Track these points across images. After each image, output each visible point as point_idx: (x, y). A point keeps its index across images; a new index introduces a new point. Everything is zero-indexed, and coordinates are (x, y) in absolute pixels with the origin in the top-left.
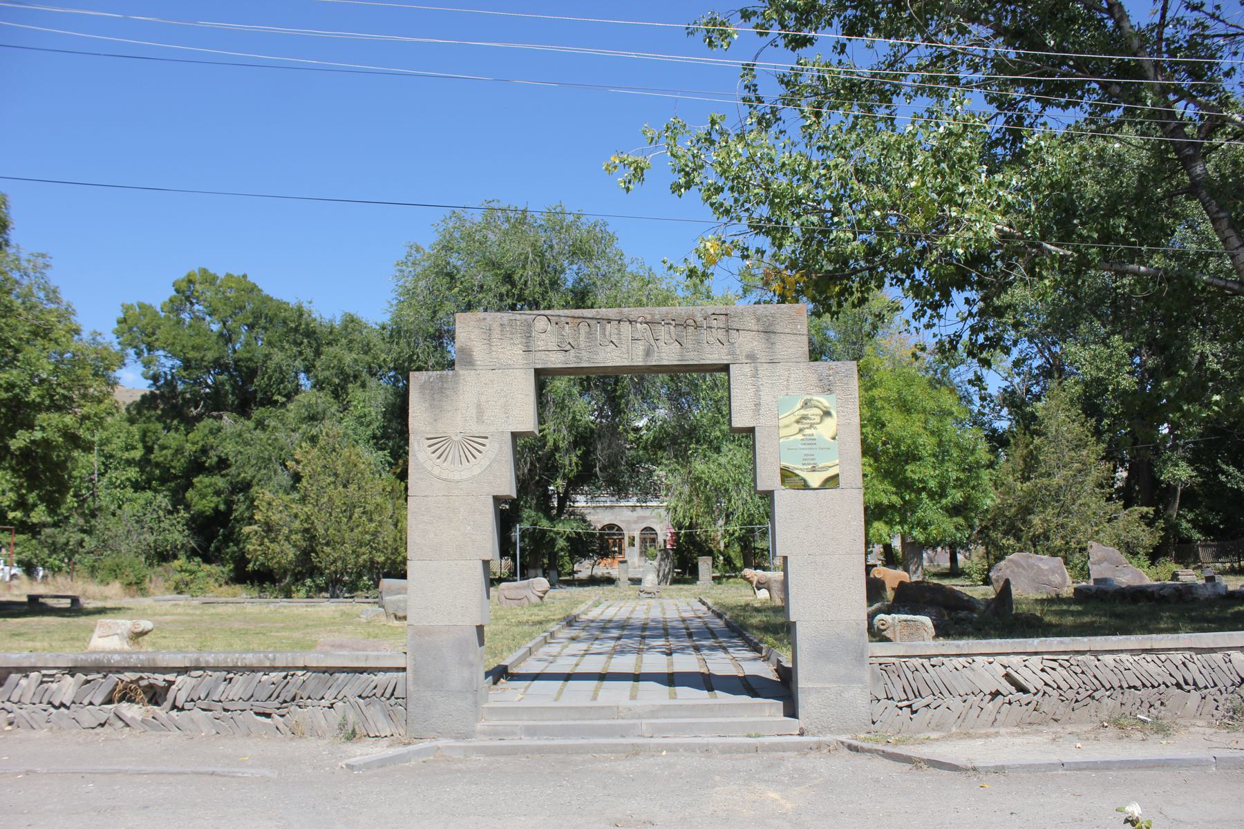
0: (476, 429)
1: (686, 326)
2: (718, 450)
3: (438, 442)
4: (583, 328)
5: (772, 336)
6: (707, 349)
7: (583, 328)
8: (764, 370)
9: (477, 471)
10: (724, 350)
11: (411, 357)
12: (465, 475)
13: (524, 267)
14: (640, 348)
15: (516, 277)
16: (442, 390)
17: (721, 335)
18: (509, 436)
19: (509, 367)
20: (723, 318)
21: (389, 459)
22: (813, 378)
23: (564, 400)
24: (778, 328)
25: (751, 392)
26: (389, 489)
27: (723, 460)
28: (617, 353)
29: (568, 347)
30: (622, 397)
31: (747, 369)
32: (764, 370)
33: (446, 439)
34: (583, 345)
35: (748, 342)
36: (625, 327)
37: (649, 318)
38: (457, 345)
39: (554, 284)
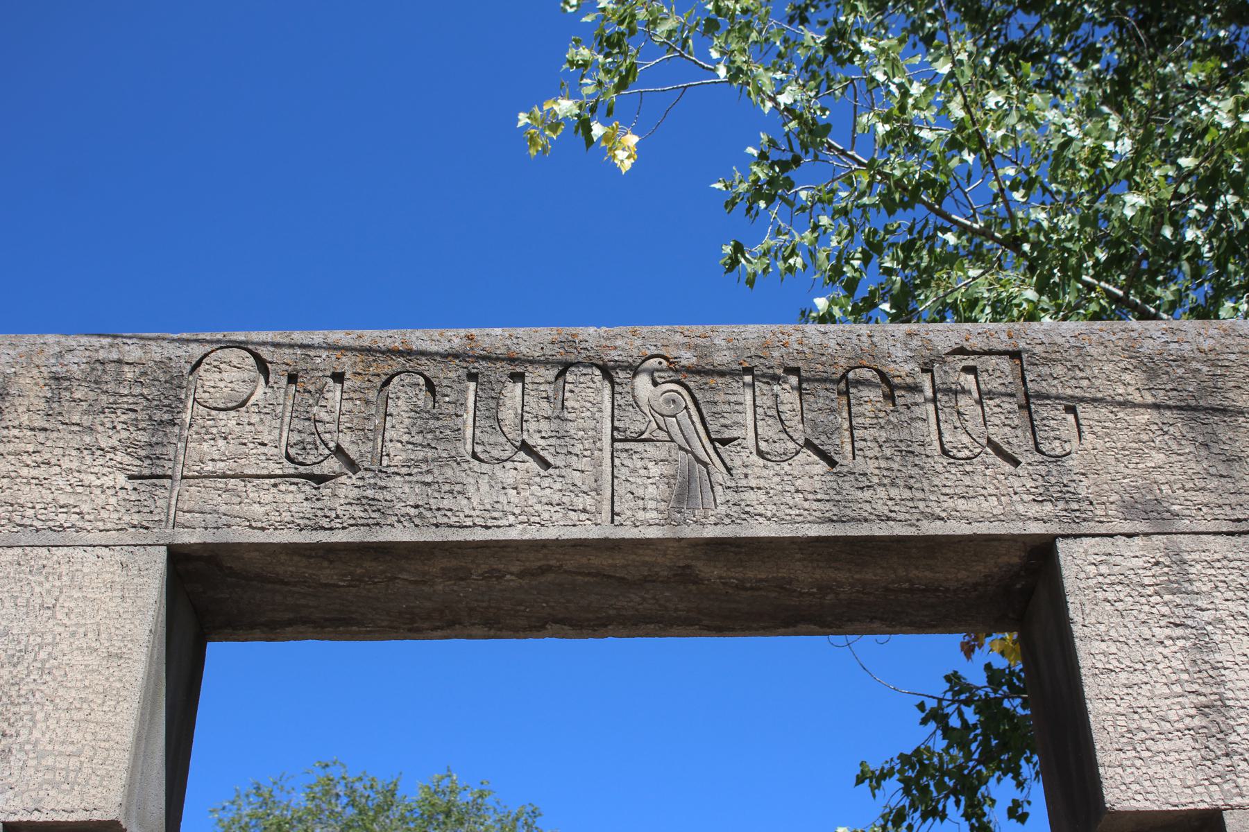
1: (845, 385)
4: (405, 398)
6: (949, 477)
7: (405, 398)
10: (1024, 480)
17: (1003, 424)
19: (54, 536)
20: (1005, 364)
25: (1173, 655)
28: (551, 488)
29: (332, 465)
31: (1134, 556)
34: (398, 454)
36: (590, 396)
37: (687, 358)
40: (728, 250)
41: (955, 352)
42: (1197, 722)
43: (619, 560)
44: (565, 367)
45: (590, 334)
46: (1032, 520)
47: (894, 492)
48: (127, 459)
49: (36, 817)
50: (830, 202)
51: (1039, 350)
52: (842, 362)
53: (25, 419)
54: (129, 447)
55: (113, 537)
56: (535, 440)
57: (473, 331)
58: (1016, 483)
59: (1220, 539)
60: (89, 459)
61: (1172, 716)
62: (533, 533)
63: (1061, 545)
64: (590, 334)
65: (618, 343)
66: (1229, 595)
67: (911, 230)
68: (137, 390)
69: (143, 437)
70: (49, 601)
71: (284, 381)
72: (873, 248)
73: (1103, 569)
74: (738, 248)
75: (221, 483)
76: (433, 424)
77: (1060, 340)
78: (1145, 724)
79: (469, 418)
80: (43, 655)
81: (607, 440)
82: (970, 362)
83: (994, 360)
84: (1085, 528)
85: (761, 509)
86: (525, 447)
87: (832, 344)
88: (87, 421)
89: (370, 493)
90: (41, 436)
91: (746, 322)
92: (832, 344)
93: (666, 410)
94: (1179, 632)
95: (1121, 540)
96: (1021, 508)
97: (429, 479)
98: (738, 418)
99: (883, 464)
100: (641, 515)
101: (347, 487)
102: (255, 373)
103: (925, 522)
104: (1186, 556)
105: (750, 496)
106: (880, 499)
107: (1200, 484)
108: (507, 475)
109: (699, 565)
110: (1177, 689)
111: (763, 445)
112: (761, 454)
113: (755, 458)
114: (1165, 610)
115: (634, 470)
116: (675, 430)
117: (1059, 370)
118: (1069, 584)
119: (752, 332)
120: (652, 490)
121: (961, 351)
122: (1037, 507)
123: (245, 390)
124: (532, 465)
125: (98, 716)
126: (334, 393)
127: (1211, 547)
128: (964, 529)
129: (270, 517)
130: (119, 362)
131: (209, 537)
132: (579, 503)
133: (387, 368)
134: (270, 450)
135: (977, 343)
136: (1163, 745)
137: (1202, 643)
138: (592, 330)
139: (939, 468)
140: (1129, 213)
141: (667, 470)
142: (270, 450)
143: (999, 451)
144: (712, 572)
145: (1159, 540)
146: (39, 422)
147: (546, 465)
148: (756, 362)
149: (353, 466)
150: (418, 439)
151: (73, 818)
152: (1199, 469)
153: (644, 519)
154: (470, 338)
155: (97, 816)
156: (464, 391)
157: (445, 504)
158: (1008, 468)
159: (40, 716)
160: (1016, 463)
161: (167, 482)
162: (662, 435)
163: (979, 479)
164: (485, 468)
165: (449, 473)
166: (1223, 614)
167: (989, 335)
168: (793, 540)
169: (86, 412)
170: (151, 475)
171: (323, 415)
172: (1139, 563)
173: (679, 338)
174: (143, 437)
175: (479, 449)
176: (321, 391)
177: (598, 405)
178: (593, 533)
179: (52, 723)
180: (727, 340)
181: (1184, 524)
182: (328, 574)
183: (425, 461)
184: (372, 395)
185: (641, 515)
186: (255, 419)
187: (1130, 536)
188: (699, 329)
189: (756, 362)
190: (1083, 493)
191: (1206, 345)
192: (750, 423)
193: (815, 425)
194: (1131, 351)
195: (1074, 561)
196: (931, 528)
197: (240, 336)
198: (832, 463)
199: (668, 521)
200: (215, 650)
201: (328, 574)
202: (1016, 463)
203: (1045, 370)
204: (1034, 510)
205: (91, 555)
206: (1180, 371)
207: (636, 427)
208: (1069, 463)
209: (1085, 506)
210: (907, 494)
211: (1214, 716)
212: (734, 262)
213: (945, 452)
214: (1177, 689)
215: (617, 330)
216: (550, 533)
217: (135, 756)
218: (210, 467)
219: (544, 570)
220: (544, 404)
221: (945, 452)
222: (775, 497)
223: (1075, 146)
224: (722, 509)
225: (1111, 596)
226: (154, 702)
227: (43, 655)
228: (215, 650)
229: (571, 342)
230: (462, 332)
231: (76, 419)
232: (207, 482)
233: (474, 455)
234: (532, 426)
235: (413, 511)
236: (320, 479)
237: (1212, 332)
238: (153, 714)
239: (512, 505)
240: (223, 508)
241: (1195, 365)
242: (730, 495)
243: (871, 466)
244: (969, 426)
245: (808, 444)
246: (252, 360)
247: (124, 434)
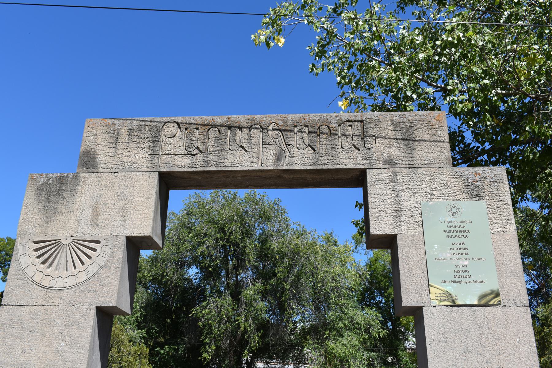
0: (88, 232)
2: (342, 336)
3: (47, 249)
4: (213, 133)
5: (411, 142)
6: (342, 154)
8: (403, 174)
9: (83, 277)
10: (360, 155)
11: (163, 274)
12: (70, 282)
13: (231, 224)
14: (270, 154)
15: (226, 229)
16: (59, 193)
17: (357, 141)
18: (123, 241)
19: (132, 170)
20: (359, 124)
21: (145, 335)
22: (459, 184)
23: (251, 302)
24: (418, 135)
25: (391, 198)
26: (139, 353)
27: (345, 342)
28: (247, 157)
29: (196, 151)
30: (285, 301)
31: (385, 174)
32: (403, 174)
33: (57, 243)
34: (211, 149)
35: (385, 148)
39: (248, 234)
40: (311, 66)
41: (347, 121)
42: (394, 214)
43: (263, 174)
44: (250, 129)
45: (258, 117)
46: (361, 164)
47: (329, 158)
48: (148, 150)
49: (132, 235)
50: (337, 55)
51: (368, 120)
52: (319, 124)
53: (123, 140)
54: (148, 147)
56: (244, 145)
57: (230, 116)
58: (358, 155)
59: (406, 169)
60: (139, 150)
61: (388, 212)
62: (243, 168)
63: (368, 171)
64: (258, 117)
65: (265, 119)
66: (406, 183)
67: (362, 61)
68: (149, 133)
69: (151, 145)
70: (132, 185)
71: (184, 130)
72: (350, 67)
73: (377, 177)
74: (314, 66)
75: (170, 156)
76: (219, 141)
77: (374, 118)
78: (382, 215)
79: (228, 139)
80: (132, 198)
81: (261, 145)
82: (350, 124)
83: (356, 123)
85: (296, 162)
86: (242, 147)
87: (317, 119)
88: (138, 140)
89: (205, 158)
90: (128, 144)
91: (296, 113)
92: (317, 119)
93: (276, 137)
94: (393, 192)
96: (359, 162)
97: (219, 155)
98: (293, 139)
99: (327, 150)
100: (268, 164)
101: (200, 157)
102: (177, 128)
103: (335, 165)
104: (397, 174)
105: (294, 159)
106: (325, 159)
107: (403, 155)
108: (237, 154)
109: (283, 175)
110: (391, 206)
111: (298, 146)
112: (298, 148)
113: (296, 149)
114: (390, 187)
115: (267, 152)
116: (277, 142)
117: (372, 125)
118: (368, 181)
119: (297, 116)
120: (271, 157)
121: (349, 121)
122: (363, 161)
123: (175, 132)
124: (243, 151)
125: (145, 212)
126: (196, 133)
127: (404, 171)
128: (345, 167)
129: (182, 164)
130: (145, 125)
131: (168, 170)
132: (254, 160)
133: (209, 127)
134: (181, 148)
135: (353, 118)
136: (386, 219)
137: (398, 195)
138: (258, 116)
139: (340, 151)
140: (421, 59)
141: (275, 152)
142: (181, 148)
143: (355, 147)
144: (286, 176)
145: (391, 170)
146: (127, 141)
147: (246, 151)
148: (298, 124)
149: (201, 152)
150: (216, 145)
151: (140, 235)
152: (403, 151)
153: (269, 165)
154: (229, 118)
155: (146, 235)
156: (227, 132)
157: (223, 161)
158: (357, 151)
159: (132, 212)
160: (359, 150)
161: (157, 156)
162: (274, 143)
163: (349, 154)
164: (232, 152)
165: (223, 153)
166: (404, 188)
167: (356, 116)
168: (304, 170)
169: (138, 138)
170: (154, 154)
171: (194, 139)
172: (386, 175)
173: (279, 118)
174: (151, 145)
175: (230, 147)
176: (193, 132)
177: (259, 136)
178: (257, 168)
179: (135, 214)
180: (292, 117)
181: (398, 166)
182: (196, 177)
183: (218, 150)
184: (205, 133)
185: (268, 164)
186: (178, 140)
187: (384, 168)
188: (284, 115)
189: (298, 124)
190: (374, 158)
191: (410, 119)
192: (295, 140)
193: (311, 140)
194: (391, 120)
195: (371, 175)
197: (173, 119)
198: (315, 150)
199: (274, 165)
200: (172, 192)
201: (196, 177)
202: (359, 150)
203: (369, 126)
204: (362, 162)
205: (141, 174)
206: (403, 126)
207: (268, 141)
208: (372, 150)
209: (375, 161)
210: (332, 158)
211: (398, 213)
212: (312, 70)
213: (342, 147)
214: (391, 206)
215: (264, 116)
216: (247, 168)
217: (154, 221)
218: (167, 152)
219: (246, 176)
220: (246, 136)
221: (342, 147)
222: (300, 159)
223: (405, 41)
224: (287, 162)
225: (378, 184)
226: (157, 208)
227: (132, 198)
228: (172, 192)
229: (253, 119)
230: (227, 117)
231: (135, 140)
232: (167, 156)
233: (230, 149)
234: (243, 141)
235: (215, 163)
236: (194, 155)
237: (412, 115)
238: (157, 210)
239: (239, 161)
240: (171, 162)
241: (407, 124)
242: (290, 159)
243: (324, 151)
244: (349, 140)
245: (309, 145)
246: (176, 125)
247: (147, 144)
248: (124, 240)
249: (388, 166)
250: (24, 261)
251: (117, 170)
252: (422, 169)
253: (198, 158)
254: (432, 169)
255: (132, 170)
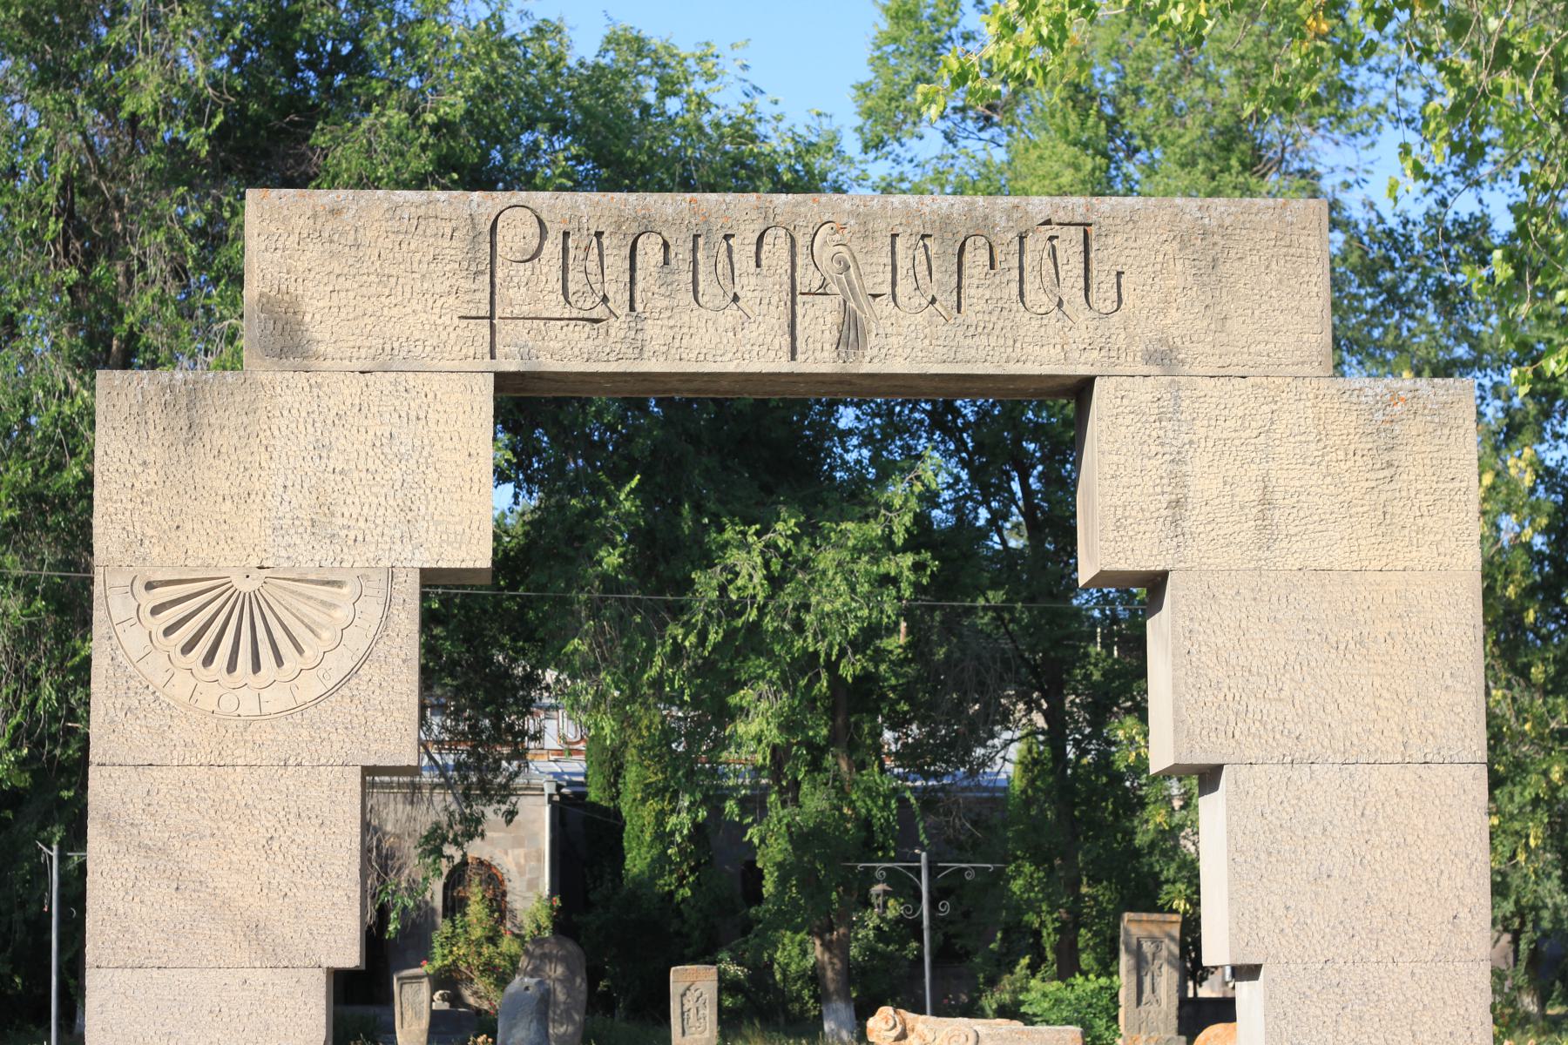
9: (311, 687)
14: (819, 320)
31: (1144, 392)
38: (252, 290)
55: (456, 365)
84: (1118, 370)
95: (1139, 380)
121: (1048, 222)
155: (478, 565)
196: (1013, 369)
218: (516, 312)
248: (415, 580)
249: (1155, 370)
250: (134, 640)
251: (367, 366)
252: (1250, 381)
253: (612, 332)
254: (1279, 381)
255: (415, 365)
